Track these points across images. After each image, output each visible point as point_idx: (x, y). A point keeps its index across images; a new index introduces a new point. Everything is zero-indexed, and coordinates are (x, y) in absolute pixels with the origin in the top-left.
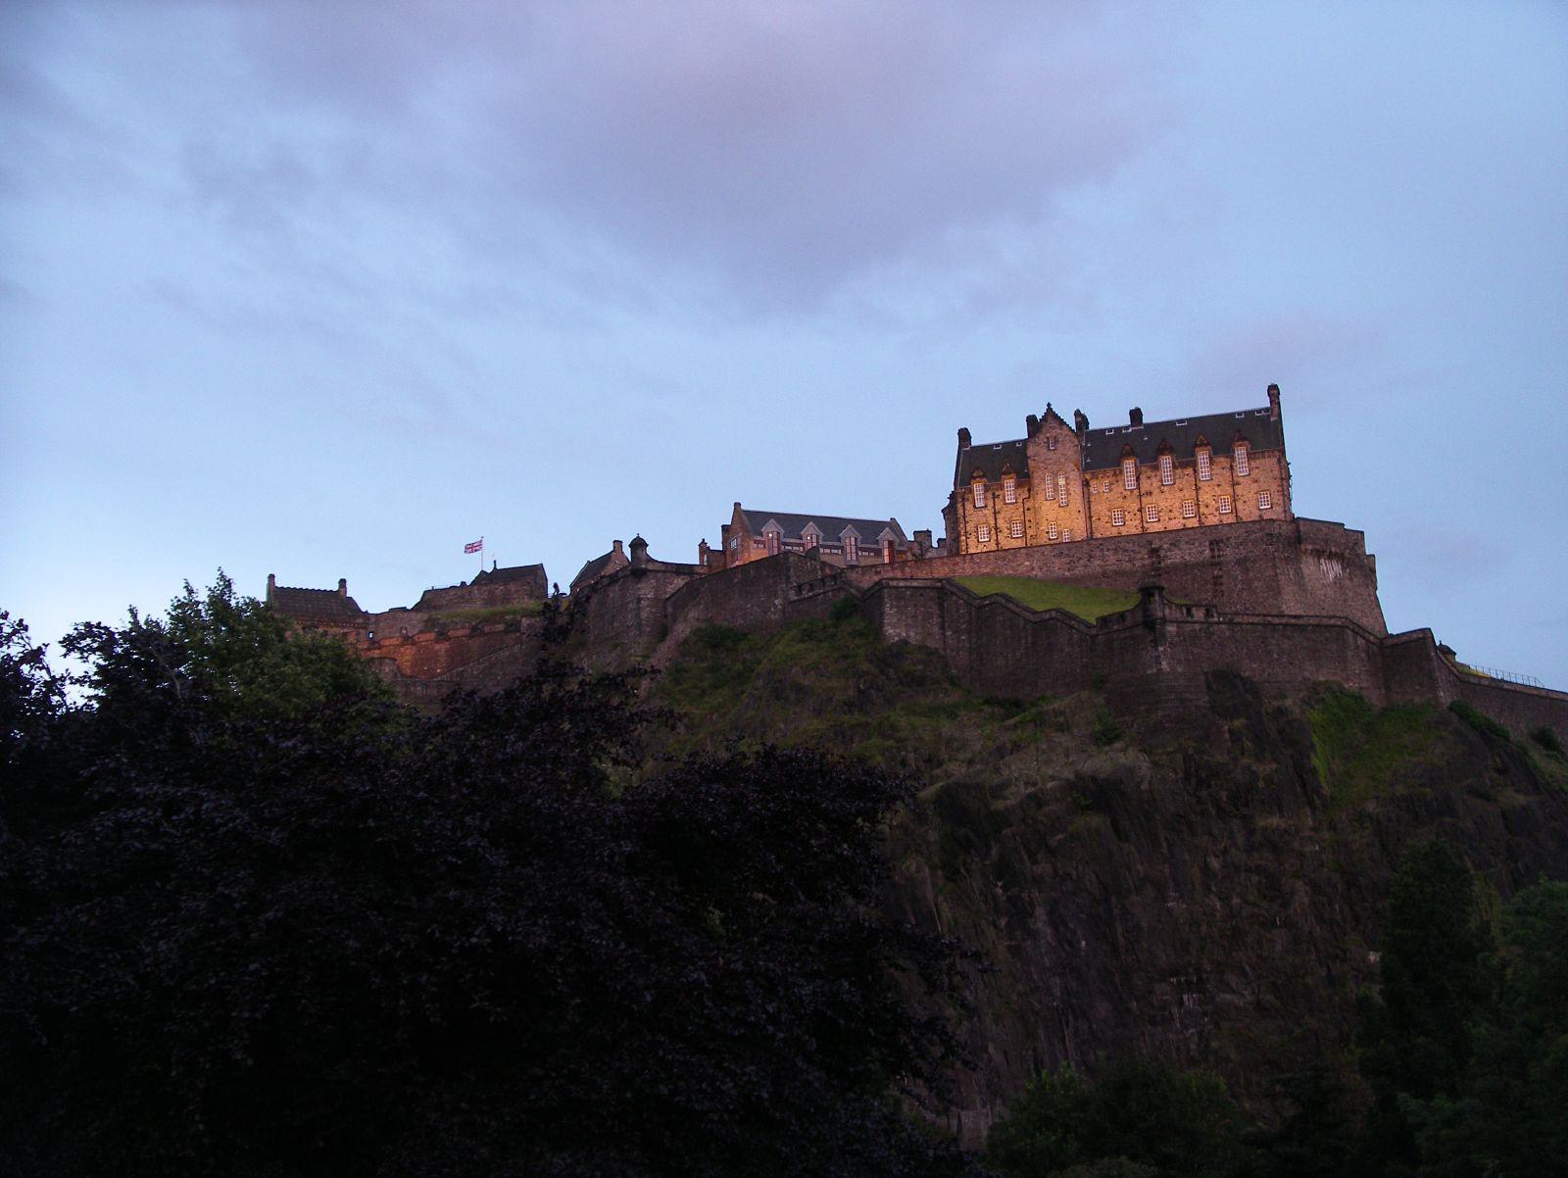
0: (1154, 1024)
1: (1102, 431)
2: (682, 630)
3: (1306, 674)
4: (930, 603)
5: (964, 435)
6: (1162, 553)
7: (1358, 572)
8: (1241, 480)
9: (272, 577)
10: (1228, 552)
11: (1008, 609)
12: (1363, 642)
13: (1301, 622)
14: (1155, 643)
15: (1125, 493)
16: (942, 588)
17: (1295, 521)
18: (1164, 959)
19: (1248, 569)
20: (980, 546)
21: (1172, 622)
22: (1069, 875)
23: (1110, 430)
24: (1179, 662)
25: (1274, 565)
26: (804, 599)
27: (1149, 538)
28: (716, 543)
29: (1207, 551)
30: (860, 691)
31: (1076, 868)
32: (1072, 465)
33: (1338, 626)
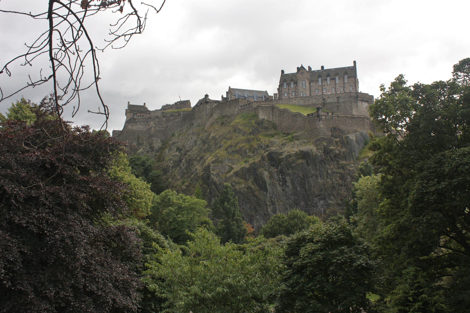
0: (314, 207)
1: (314, 71)
2: (215, 116)
5: (283, 72)
9: (129, 102)
10: (341, 99)
14: (320, 121)
17: (357, 93)
28: (225, 96)
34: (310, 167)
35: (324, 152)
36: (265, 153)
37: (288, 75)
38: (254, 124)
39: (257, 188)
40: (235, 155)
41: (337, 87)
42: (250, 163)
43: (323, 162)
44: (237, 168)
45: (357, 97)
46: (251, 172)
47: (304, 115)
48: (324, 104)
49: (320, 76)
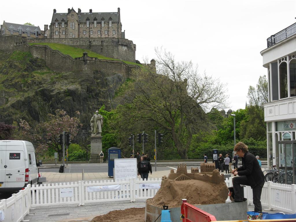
1: (83, 13)
3: (113, 72)
4: (43, 50)
5: (55, 11)
6: (92, 42)
7: (130, 49)
10: (105, 43)
11: (59, 54)
13: (113, 62)
16: (45, 48)
20: (56, 35)
22: (64, 108)
23: (85, 13)
24: (89, 68)
30: (28, 67)
31: (65, 106)
35: (87, 91)
36: (38, 89)
37: (59, 14)
38: (29, 62)
39: (31, 118)
40: (11, 89)
41: (103, 30)
42: (25, 97)
43: (85, 99)
44: (12, 100)
45: (119, 42)
46: (26, 105)
47: (72, 58)
48: (90, 46)
49: (88, 19)
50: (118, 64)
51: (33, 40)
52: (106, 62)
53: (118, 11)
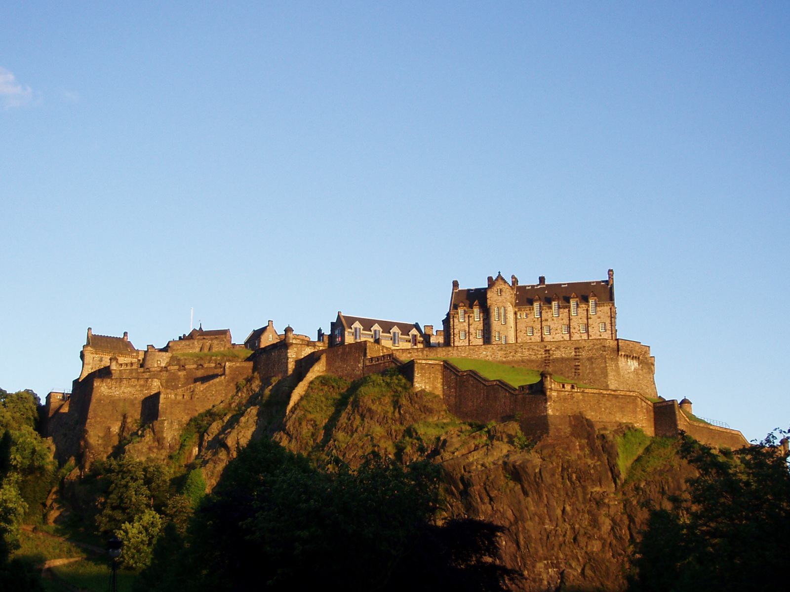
3: (618, 419)
5: (455, 284)
6: (551, 352)
7: (646, 367)
8: (592, 317)
10: (583, 353)
12: (645, 404)
15: (534, 319)
18: (542, 552)
19: (592, 363)
20: (461, 341)
21: (555, 391)
22: (500, 511)
23: (529, 286)
24: (557, 410)
25: (605, 361)
26: (374, 365)
27: (545, 344)
29: (573, 353)
31: (503, 508)
32: (509, 303)
33: (634, 396)
34: (529, 499)
50: (628, 400)
51: (410, 353)
52: (596, 395)
53: (609, 278)
